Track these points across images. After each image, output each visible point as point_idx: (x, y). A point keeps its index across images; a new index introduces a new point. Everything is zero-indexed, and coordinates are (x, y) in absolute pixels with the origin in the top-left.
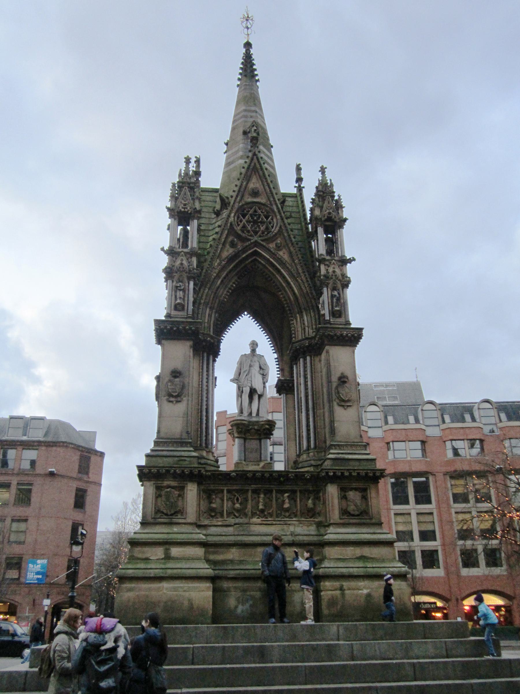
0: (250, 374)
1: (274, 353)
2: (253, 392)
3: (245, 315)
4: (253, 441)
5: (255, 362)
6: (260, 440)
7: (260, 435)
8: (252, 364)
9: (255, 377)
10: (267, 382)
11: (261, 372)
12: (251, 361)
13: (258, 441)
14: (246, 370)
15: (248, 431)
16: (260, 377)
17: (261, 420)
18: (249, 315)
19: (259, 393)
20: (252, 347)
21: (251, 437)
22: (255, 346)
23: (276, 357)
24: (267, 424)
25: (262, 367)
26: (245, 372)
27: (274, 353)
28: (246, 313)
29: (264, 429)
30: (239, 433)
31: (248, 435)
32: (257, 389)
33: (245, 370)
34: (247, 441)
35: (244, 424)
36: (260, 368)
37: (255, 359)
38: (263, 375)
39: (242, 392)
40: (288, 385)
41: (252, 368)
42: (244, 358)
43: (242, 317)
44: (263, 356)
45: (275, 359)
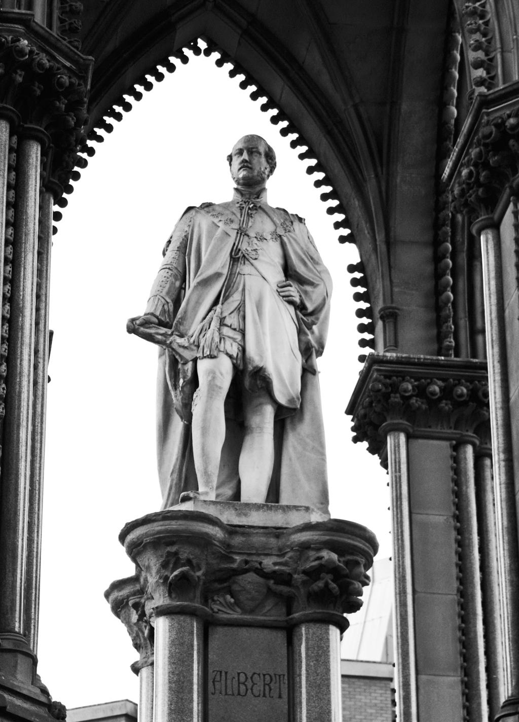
0: (236, 298)
1: (342, 239)
2: (248, 388)
3: (197, 51)
4: (244, 632)
5: (262, 239)
6: (290, 631)
7: (289, 603)
8: (244, 246)
9: (259, 307)
10: (320, 353)
11: (294, 291)
12: (242, 232)
13: (279, 638)
14: (218, 275)
15: (223, 580)
16: (287, 318)
17: (296, 519)
18: (216, 56)
19: (282, 399)
20: (245, 165)
21: (236, 615)
22: (262, 164)
23: (356, 259)
24: (332, 546)
25: (301, 269)
26: (206, 283)
27: (342, 239)
28: (202, 44)
29: (313, 574)
30: (175, 587)
31: (223, 608)
32: (271, 371)
33: (206, 273)
34: (218, 636)
35: (204, 541)
36: (288, 270)
37: (262, 225)
38: (300, 307)
39: (194, 382)
40: (421, 391)
41: (246, 269)
42: (203, 222)
43: (185, 60)
44: (301, 220)
45: (351, 268)
